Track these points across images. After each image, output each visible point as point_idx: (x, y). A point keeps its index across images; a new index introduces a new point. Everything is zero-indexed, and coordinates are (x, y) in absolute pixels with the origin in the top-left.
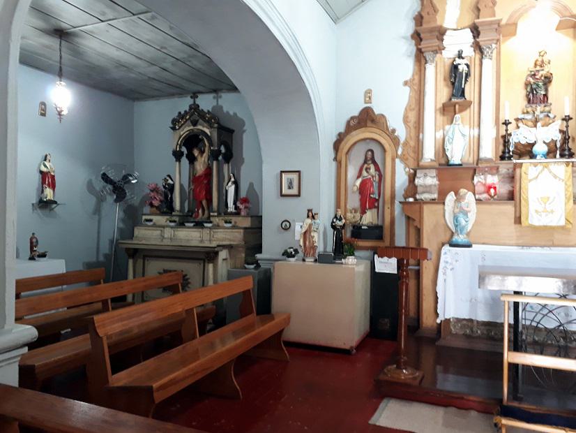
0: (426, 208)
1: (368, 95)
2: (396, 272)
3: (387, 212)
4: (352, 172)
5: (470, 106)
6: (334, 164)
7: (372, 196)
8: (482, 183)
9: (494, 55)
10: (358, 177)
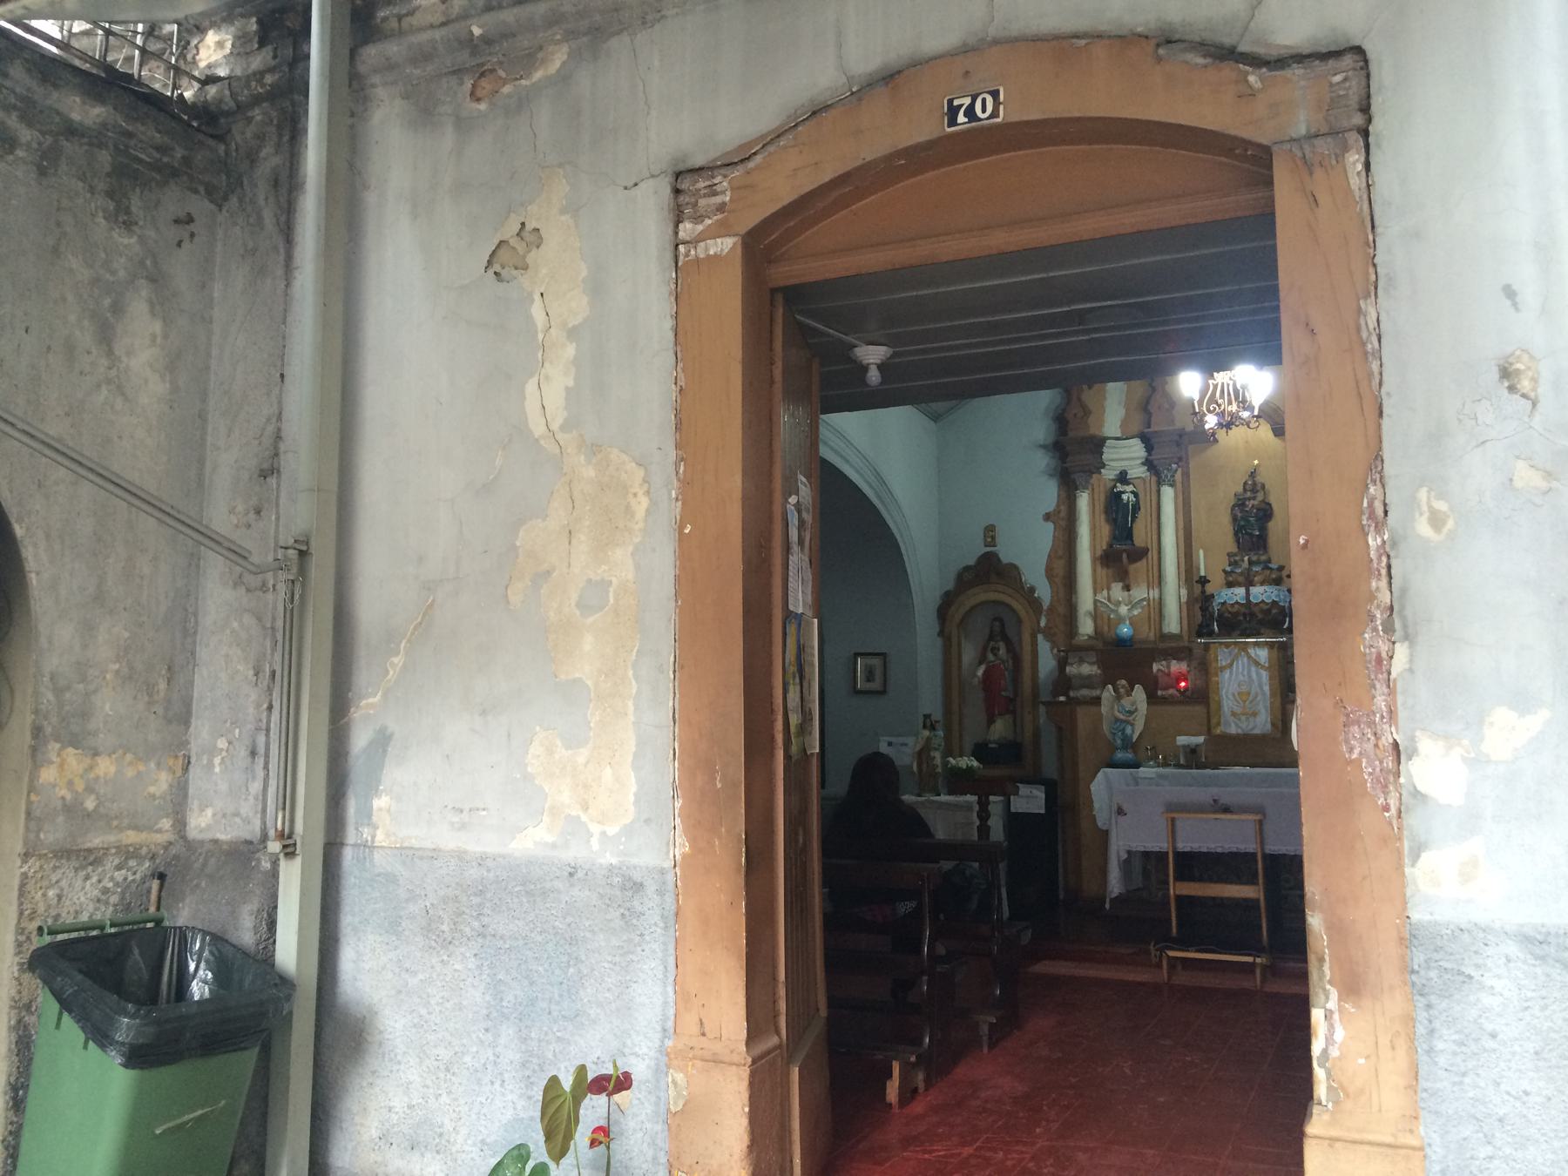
1: (990, 533)
2: (1043, 811)
5: (1147, 553)
6: (939, 642)
7: (1003, 693)
9: (1178, 476)
10: (980, 663)
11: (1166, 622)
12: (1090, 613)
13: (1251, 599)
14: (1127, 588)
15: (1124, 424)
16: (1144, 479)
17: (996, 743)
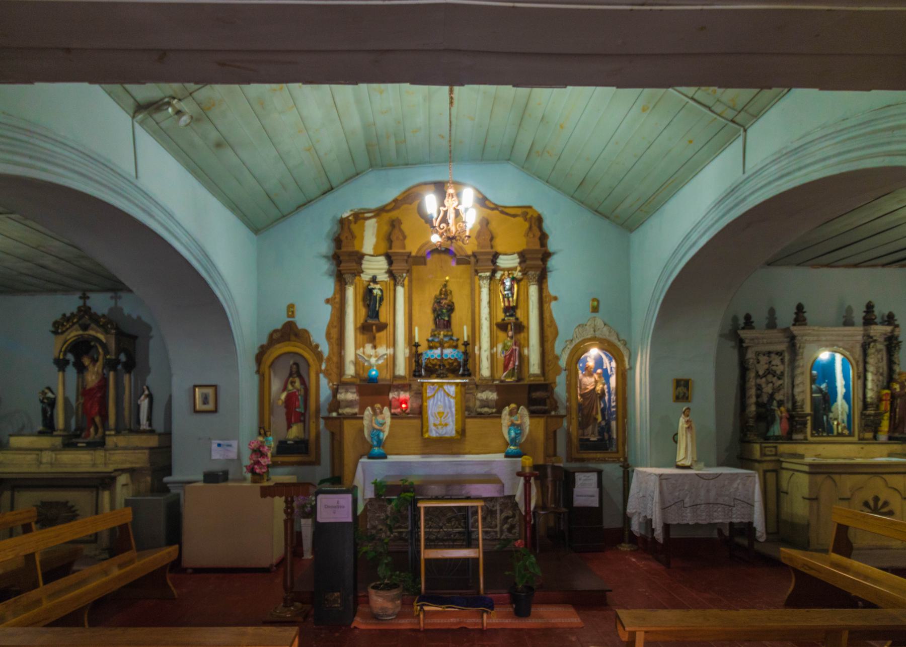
0: (347, 424)
3: (313, 426)
4: (276, 385)
6: (256, 378)
7: (297, 410)
8: (396, 399)
9: (406, 282)
11: (397, 368)
13: (444, 356)
14: (375, 347)
15: (376, 247)
16: (386, 282)
17: (292, 441)
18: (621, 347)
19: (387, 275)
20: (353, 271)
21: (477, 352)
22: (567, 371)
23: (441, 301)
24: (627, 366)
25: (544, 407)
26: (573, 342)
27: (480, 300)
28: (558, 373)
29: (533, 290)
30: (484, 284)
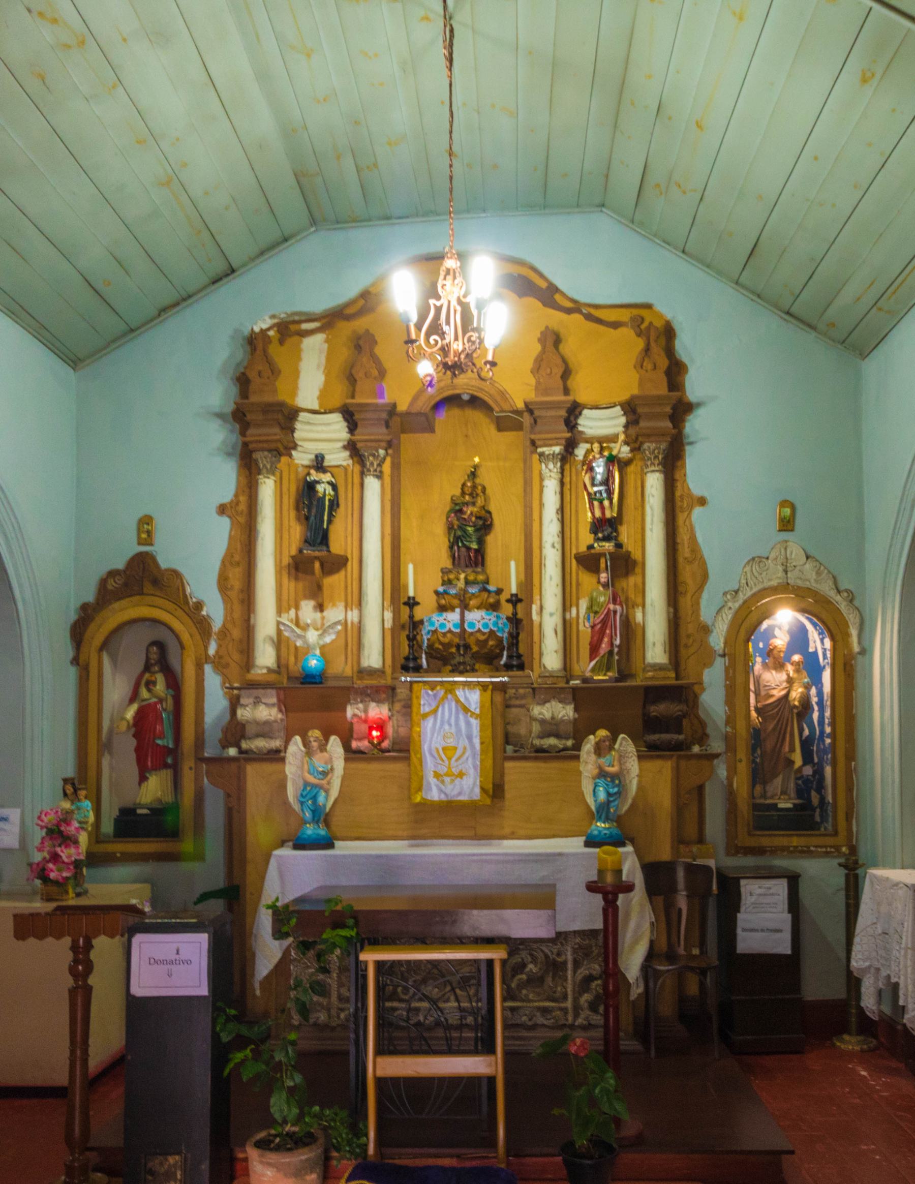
6: (73, 672)
7: (159, 742)
8: (360, 718)
9: (387, 467)
10: (132, 700)
11: (366, 652)
12: (271, 639)
13: (466, 626)
14: (320, 607)
15: (323, 395)
16: (345, 469)
17: (148, 809)
18: (843, 606)
19: (347, 454)
20: (273, 446)
21: (535, 617)
22: (727, 658)
23: (465, 509)
24: (856, 648)
25: (675, 737)
26: (740, 593)
27: (541, 505)
28: (708, 664)
29: (654, 483)
30: (550, 471)
